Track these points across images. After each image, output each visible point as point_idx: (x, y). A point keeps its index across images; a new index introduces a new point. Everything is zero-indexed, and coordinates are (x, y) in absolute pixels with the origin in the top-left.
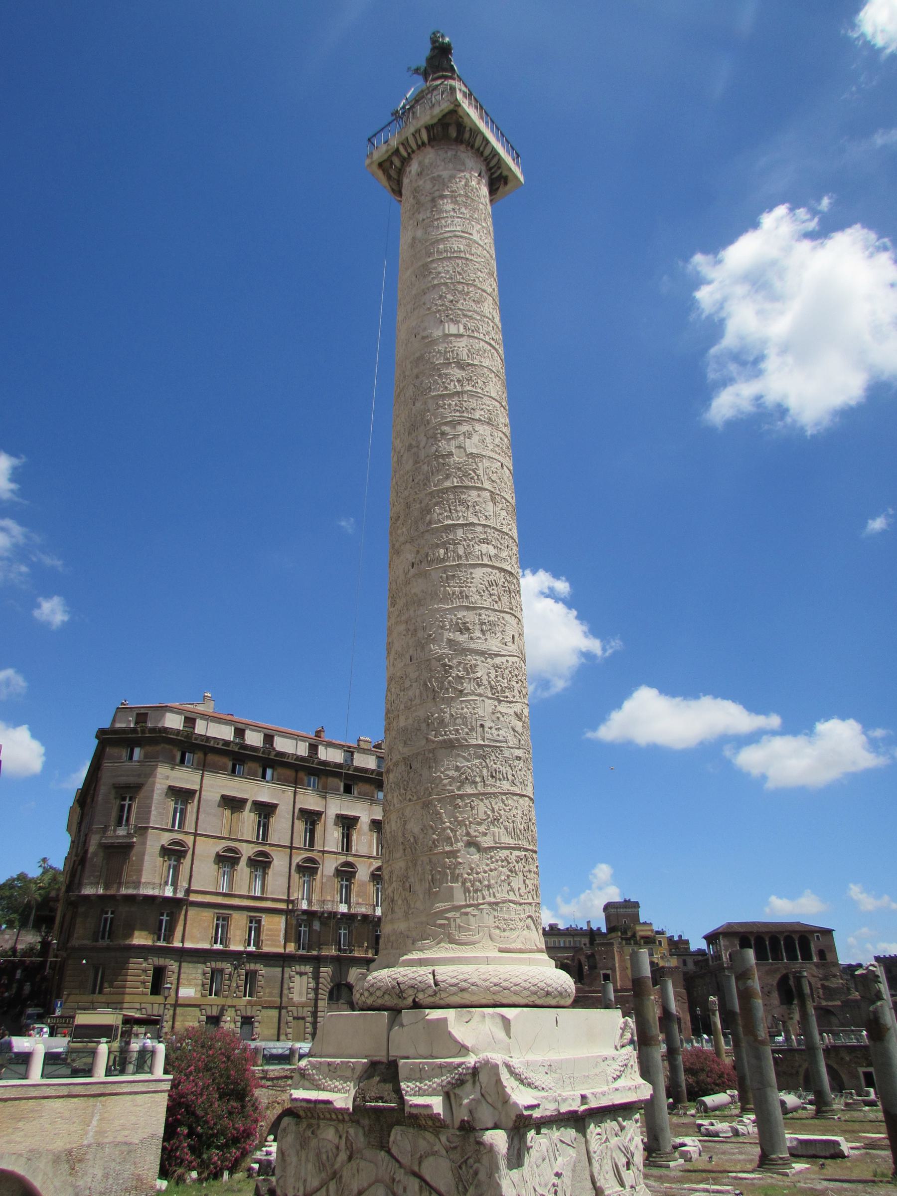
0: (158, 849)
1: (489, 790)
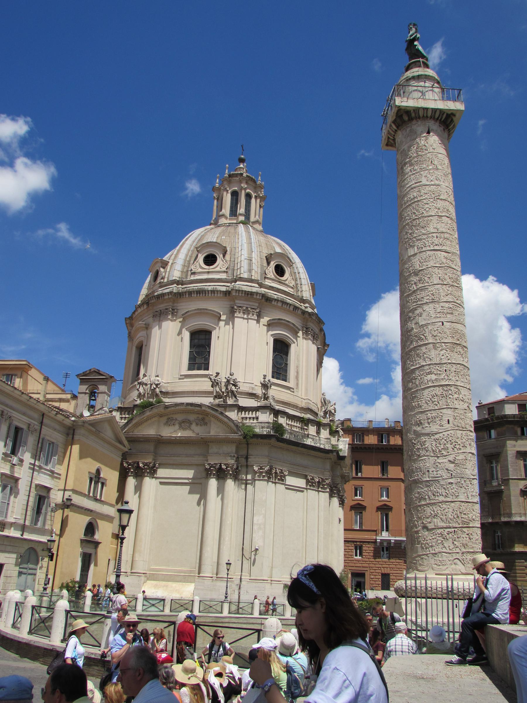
0: (518, 492)
1: (432, 501)
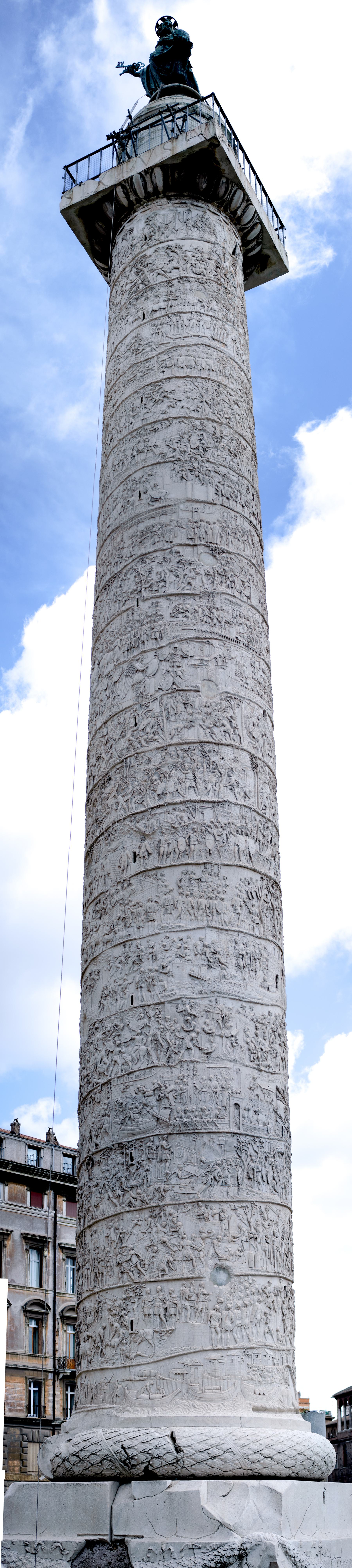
1: (243, 1196)
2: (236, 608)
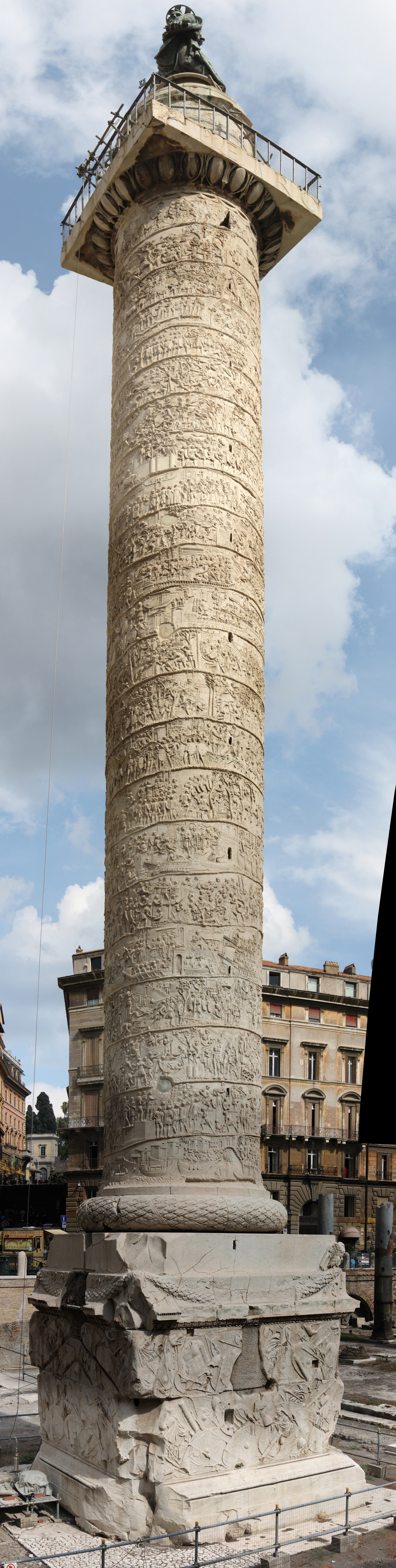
1: (184, 1024)
2: (196, 553)
